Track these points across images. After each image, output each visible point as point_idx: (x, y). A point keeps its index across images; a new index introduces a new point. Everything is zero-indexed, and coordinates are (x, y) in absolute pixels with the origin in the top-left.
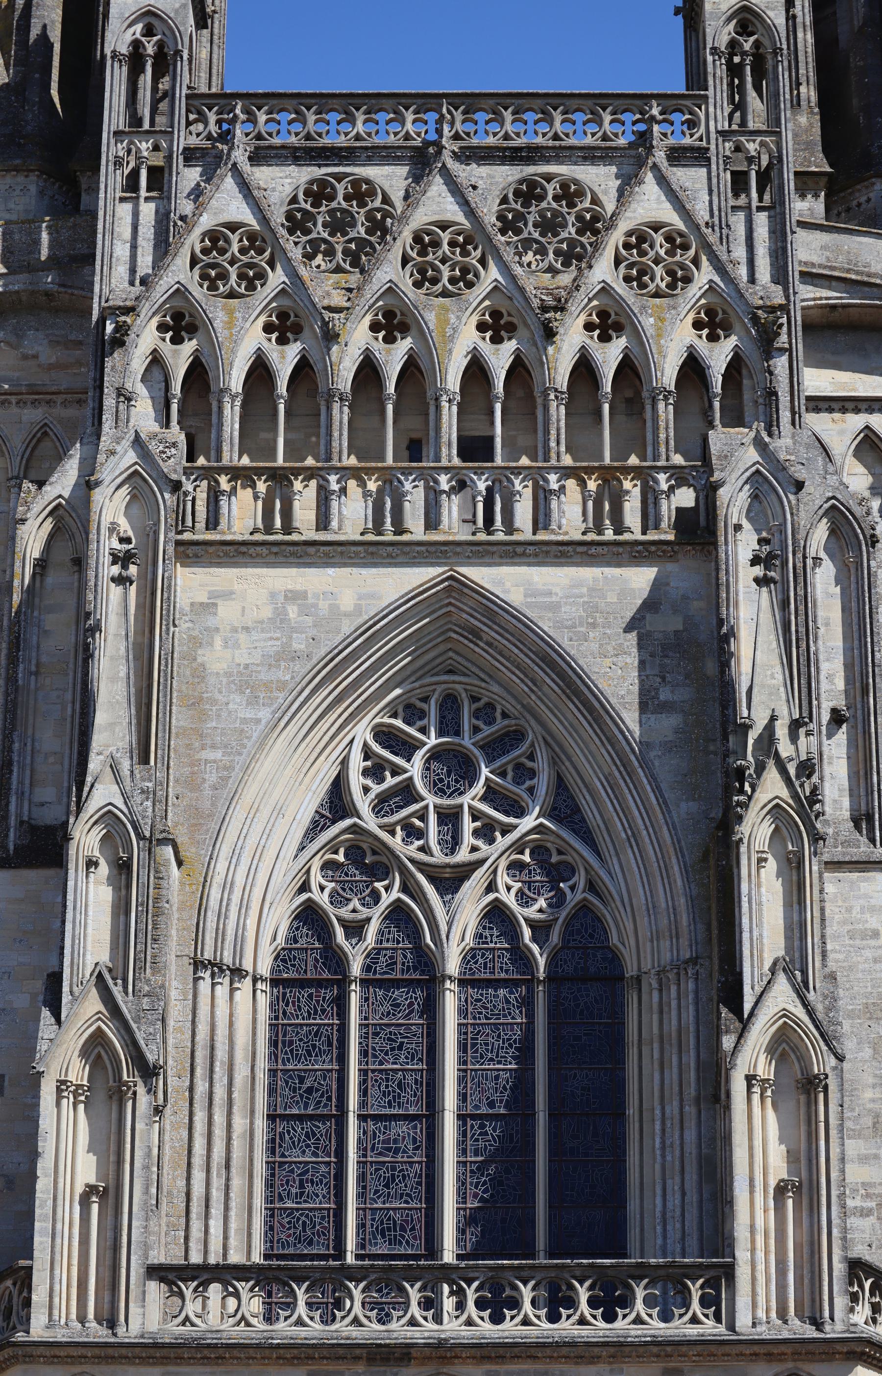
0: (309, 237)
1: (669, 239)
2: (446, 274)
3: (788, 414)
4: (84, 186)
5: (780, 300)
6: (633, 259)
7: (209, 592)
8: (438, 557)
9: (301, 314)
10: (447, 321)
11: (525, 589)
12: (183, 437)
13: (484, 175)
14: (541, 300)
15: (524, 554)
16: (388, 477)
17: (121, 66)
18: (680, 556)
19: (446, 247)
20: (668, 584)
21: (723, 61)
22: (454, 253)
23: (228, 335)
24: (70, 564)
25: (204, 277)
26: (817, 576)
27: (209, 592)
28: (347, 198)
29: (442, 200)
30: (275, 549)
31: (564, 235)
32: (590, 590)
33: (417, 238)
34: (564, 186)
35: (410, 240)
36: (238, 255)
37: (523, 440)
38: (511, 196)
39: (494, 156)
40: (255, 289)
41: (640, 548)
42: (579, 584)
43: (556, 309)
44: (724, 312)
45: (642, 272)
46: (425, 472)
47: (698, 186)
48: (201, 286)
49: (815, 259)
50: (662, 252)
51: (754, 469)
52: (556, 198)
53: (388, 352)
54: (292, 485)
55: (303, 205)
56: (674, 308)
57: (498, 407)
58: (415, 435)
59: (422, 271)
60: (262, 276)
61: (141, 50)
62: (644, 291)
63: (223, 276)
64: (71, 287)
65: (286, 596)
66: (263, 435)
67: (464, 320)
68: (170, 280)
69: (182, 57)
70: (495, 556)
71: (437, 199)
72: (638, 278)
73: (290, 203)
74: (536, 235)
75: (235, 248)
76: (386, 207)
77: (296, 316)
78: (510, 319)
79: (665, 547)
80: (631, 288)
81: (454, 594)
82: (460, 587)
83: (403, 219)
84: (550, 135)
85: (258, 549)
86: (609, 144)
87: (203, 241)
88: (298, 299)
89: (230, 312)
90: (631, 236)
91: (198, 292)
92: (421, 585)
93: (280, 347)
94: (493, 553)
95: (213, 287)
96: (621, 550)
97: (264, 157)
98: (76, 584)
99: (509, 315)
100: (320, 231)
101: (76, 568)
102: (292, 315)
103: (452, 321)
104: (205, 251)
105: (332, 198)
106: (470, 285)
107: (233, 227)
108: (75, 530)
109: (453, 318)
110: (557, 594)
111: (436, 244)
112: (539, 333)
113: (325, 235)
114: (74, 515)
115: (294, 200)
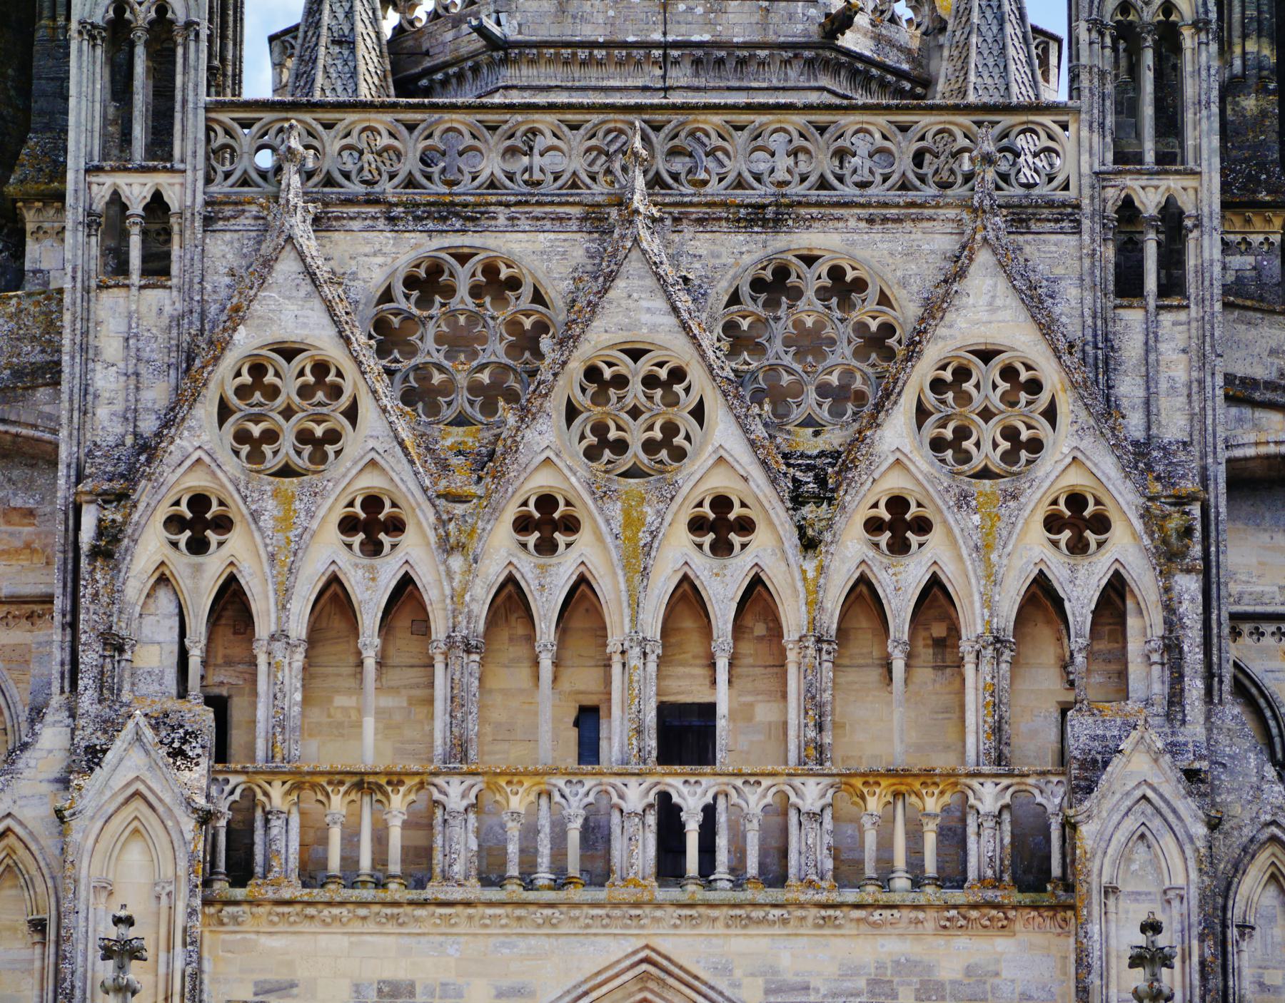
0: (413, 362)
1: (1009, 373)
2: (636, 435)
3: (1199, 684)
4: (30, 227)
5: (1189, 485)
6: (950, 411)
7: (256, 984)
8: (627, 927)
9: (401, 502)
10: (641, 521)
11: (767, 982)
12: (209, 715)
13: (703, 252)
14: (795, 480)
15: (763, 921)
16: (544, 787)
17: (94, 46)
18: (1018, 926)
19: (636, 388)
20: (997, 974)
21: (1108, 41)
22: (650, 398)
23: (283, 543)
24: (26, 928)
25: (242, 436)
26: (1245, 956)
27: (256, 984)
28: (476, 292)
29: (632, 305)
30: (362, 911)
31: (831, 360)
32: (873, 982)
33: (592, 373)
34: (836, 273)
35: (579, 375)
36: (297, 399)
37: (765, 712)
38: (746, 290)
39: (720, 219)
40: (324, 459)
41: (953, 913)
42: (854, 972)
43: (819, 500)
44: (1098, 502)
45: (963, 433)
46: (605, 780)
47: (1059, 271)
48: (237, 453)
49: (1260, 373)
50: (995, 398)
51: (1138, 794)
52: (823, 293)
53: (543, 568)
54: (389, 801)
55: (402, 304)
56: (1015, 497)
57: (722, 664)
58: (589, 701)
59: (600, 429)
60: (333, 436)
61: (128, 15)
62: (965, 467)
63: (271, 436)
64: (14, 423)
65: (380, 991)
66: (341, 701)
67: (668, 519)
68: (185, 443)
69: (197, 35)
70: (720, 924)
71: (624, 303)
72: (956, 444)
73: (379, 303)
74: (788, 360)
75: (289, 390)
76: (540, 308)
77: (394, 505)
78: (744, 511)
79: (994, 912)
80: (943, 461)
81: (651, 985)
82: (662, 975)
83: (567, 341)
84: (813, 179)
85: (336, 911)
86: (911, 196)
87: (238, 374)
88: (396, 479)
89: (286, 500)
90: (944, 368)
91: (233, 467)
92: (599, 973)
93: (367, 561)
94: (715, 920)
95: (256, 456)
96: (921, 915)
97: (337, 218)
98: (37, 964)
99: (743, 505)
100: (429, 349)
101: (37, 938)
102: (387, 503)
103: (649, 519)
104: (242, 392)
105: (449, 291)
106: (679, 455)
107: (289, 353)
108: (34, 871)
109: (650, 513)
110: (817, 990)
111: (621, 381)
112: (791, 539)
113: (439, 358)
114: (33, 847)
115: (387, 296)
